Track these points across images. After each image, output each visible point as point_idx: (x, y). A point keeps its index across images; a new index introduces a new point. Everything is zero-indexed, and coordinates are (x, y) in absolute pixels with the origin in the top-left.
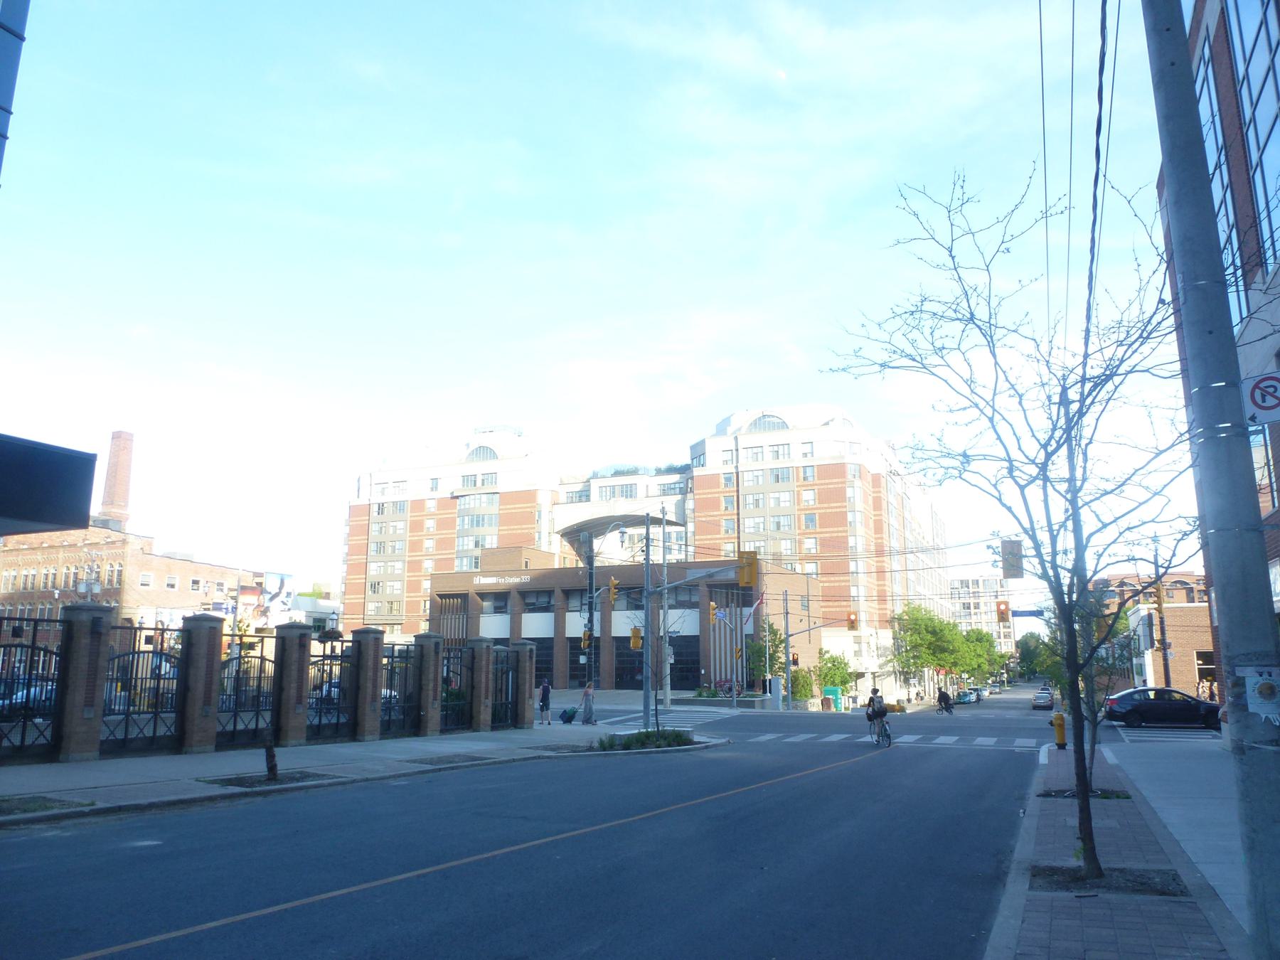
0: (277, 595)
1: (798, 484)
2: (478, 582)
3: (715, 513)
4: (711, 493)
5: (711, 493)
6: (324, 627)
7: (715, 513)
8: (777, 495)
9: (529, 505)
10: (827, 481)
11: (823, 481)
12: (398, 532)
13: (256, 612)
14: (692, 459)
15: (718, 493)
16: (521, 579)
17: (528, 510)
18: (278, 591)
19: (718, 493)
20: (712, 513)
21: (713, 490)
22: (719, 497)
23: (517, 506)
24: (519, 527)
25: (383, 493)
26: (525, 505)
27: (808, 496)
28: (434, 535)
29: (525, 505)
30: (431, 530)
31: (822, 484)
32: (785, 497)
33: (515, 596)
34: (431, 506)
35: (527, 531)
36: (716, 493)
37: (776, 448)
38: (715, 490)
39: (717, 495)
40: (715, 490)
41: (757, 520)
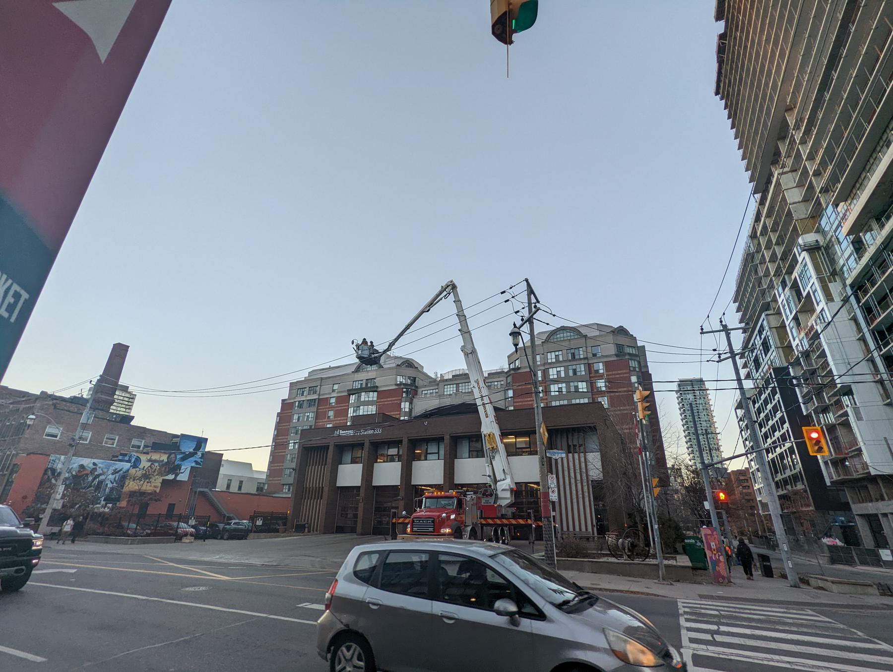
0: (192, 455)
1: (591, 375)
3: (529, 399)
6: (150, 466)
7: (529, 399)
8: (576, 384)
9: (396, 398)
10: (614, 372)
11: (611, 373)
12: (310, 419)
13: (163, 469)
14: (510, 365)
17: (396, 402)
18: (191, 450)
20: (526, 399)
22: (531, 388)
23: (389, 399)
25: (303, 395)
27: (601, 384)
28: (333, 421)
30: (331, 417)
32: (583, 386)
33: (367, 445)
34: (333, 401)
37: (572, 351)
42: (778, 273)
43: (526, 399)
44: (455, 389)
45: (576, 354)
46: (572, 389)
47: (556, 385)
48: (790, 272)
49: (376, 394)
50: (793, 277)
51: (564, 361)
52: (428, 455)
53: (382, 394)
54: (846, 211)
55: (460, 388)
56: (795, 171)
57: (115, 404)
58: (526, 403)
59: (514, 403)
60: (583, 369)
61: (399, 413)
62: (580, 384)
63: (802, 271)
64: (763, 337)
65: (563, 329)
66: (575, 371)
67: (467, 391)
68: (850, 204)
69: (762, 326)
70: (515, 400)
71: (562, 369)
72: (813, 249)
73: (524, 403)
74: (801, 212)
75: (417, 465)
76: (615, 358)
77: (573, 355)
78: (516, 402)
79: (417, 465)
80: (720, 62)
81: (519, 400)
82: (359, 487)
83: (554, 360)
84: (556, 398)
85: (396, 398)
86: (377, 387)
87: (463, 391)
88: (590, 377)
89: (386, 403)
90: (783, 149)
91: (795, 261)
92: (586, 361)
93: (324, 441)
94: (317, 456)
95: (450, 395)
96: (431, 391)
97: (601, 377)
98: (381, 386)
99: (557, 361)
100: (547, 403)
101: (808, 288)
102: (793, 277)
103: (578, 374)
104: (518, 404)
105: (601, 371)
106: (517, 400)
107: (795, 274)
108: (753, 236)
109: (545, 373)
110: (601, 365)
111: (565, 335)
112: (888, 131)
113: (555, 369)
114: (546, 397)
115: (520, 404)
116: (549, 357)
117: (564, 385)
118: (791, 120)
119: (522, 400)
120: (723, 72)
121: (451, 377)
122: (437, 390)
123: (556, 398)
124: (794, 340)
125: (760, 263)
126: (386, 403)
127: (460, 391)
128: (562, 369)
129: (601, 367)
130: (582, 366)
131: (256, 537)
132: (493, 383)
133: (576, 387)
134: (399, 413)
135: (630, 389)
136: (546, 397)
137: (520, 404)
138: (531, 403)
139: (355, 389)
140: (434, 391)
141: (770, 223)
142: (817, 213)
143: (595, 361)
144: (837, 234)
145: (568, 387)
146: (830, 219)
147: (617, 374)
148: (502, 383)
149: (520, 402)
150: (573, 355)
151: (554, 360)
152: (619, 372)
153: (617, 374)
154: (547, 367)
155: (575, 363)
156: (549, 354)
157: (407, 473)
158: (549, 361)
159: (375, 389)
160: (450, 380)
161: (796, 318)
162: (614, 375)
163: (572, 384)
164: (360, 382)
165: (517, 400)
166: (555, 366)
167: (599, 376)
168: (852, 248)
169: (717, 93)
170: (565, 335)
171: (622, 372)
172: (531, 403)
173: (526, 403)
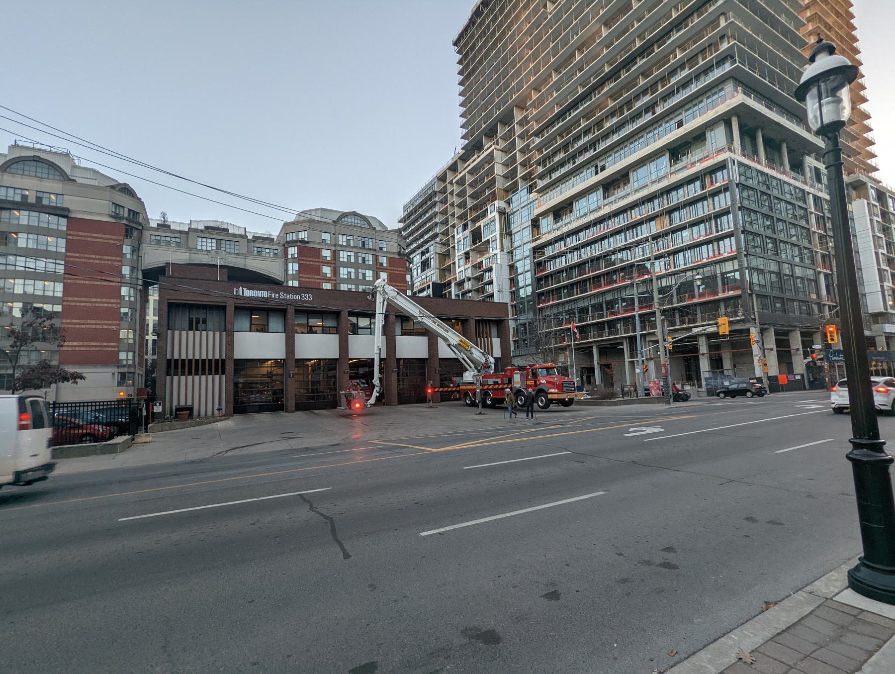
2: (240, 293)
4: (313, 261)
5: (313, 261)
8: (364, 271)
9: (113, 237)
10: (395, 268)
11: (392, 268)
15: (319, 262)
16: (301, 297)
19: (319, 262)
20: (313, 276)
21: (314, 260)
24: (100, 257)
26: (108, 237)
29: (108, 237)
31: (392, 270)
35: (110, 263)
36: (317, 262)
38: (316, 260)
39: (318, 264)
40: (316, 260)
41: (350, 286)
42: (462, 217)
43: (313, 276)
44: (214, 245)
45: (366, 243)
46: (361, 277)
47: (345, 269)
48: (474, 221)
49: (63, 221)
50: (477, 225)
51: (354, 247)
52: (359, 330)
53: (75, 224)
54: (536, 199)
55: (223, 246)
56: (506, 152)
57: (297, 213)
58: (313, 280)
59: (300, 277)
60: (371, 259)
61: (119, 259)
62: (367, 271)
63: (488, 224)
64: (424, 258)
65: (354, 214)
66: (364, 259)
67: (204, 248)
68: (541, 197)
69: (428, 249)
70: (301, 275)
71: (352, 254)
72: (502, 212)
73: (311, 280)
74: (500, 184)
75: (352, 339)
76: (397, 256)
77: (364, 243)
78: (303, 277)
79: (352, 339)
80: (472, 22)
81: (306, 276)
82: (427, 359)
83: (345, 244)
84: (345, 281)
85: (113, 237)
86: (68, 210)
87: (228, 250)
88: (377, 268)
89: (89, 239)
90: (501, 131)
91: (484, 215)
92: (374, 253)
93: (222, 300)
94: (483, 327)
95: (207, 251)
96: (168, 239)
97: (384, 270)
98: (76, 211)
99: (348, 245)
100: (335, 285)
101: (489, 237)
102: (477, 225)
103: (367, 262)
104: (304, 279)
105: (385, 265)
106: (303, 275)
107: (481, 223)
108: (442, 178)
109: (335, 254)
110: (385, 259)
111: (356, 221)
112: (585, 168)
113: (345, 253)
114: (335, 278)
115: (307, 280)
116: (340, 239)
117: (353, 270)
118: (518, 116)
119: (309, 276)
120: (469, 33)
121: (203, 228)
122: (178, 240)
123: (345, 281)
124: (459, 267)
125: (441, 202)
126: (89, 239)
127: (222, 249)
128: (352, 254)
129: (384, 260)
130: (371, 256)
131: (167, 428)
132: (263, 250)
133: (364, 275)
134: (119, 259)
135: (405, 285)
136: (335, 278)
137: (307, 280)
138: (318, 281)
139: (9, 202)
140: (173, 240)
141: (470, 179)
142: (513, 189)
143: (381, 254)
144: (522, 210)
145: (357, 273)
146: (521, 197)
147: (398, 270)
148: (276, 252)
149: (307, 278)
150: (364, 243)
151: (345, 244)
152: (399, 269)
153: (398, 270)
154: (338, 248)
155: (365, 251)
156: (340, 236)
157: (344, 346)
158: (341, 243)
159: (66, 213)
160: (201, 231)
161: (467, 254)
162: (395, 270)
163: (360, 271)
164: (19, 191)
165: (303, 275)
166: (348, 249)
167: (380, 269)
168: (530, 224)
169: (455, 44)
170: (349, 220)
171: (401, 269)
172: (318, 281)
173: (313, 280)
